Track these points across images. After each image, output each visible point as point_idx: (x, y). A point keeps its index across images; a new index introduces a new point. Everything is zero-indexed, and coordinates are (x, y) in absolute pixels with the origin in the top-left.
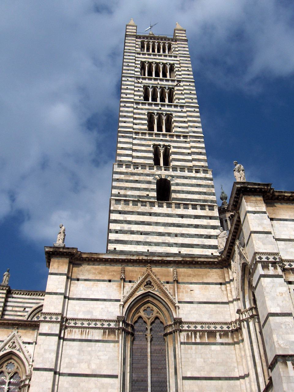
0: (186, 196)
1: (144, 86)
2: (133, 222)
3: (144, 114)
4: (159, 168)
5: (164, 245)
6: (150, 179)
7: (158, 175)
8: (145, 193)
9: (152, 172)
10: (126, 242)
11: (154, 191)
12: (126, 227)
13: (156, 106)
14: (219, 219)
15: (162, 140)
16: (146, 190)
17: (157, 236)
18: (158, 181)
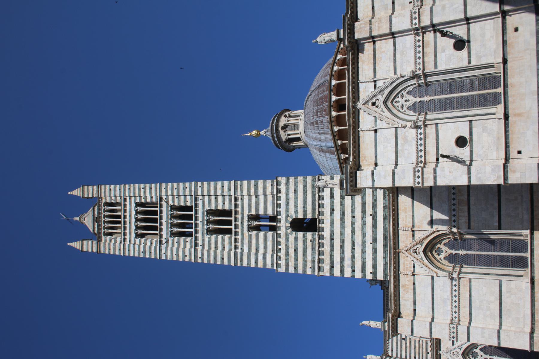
1: (171, 236)
2: (342, 256)
3: (210, 239)
4: (279, 228)
6: (292, 238)
8: (309, 244)
10: (364, 263)
12: (347, 262)
13: (198, 226)
15: (242, 223)
17: (355, 234)
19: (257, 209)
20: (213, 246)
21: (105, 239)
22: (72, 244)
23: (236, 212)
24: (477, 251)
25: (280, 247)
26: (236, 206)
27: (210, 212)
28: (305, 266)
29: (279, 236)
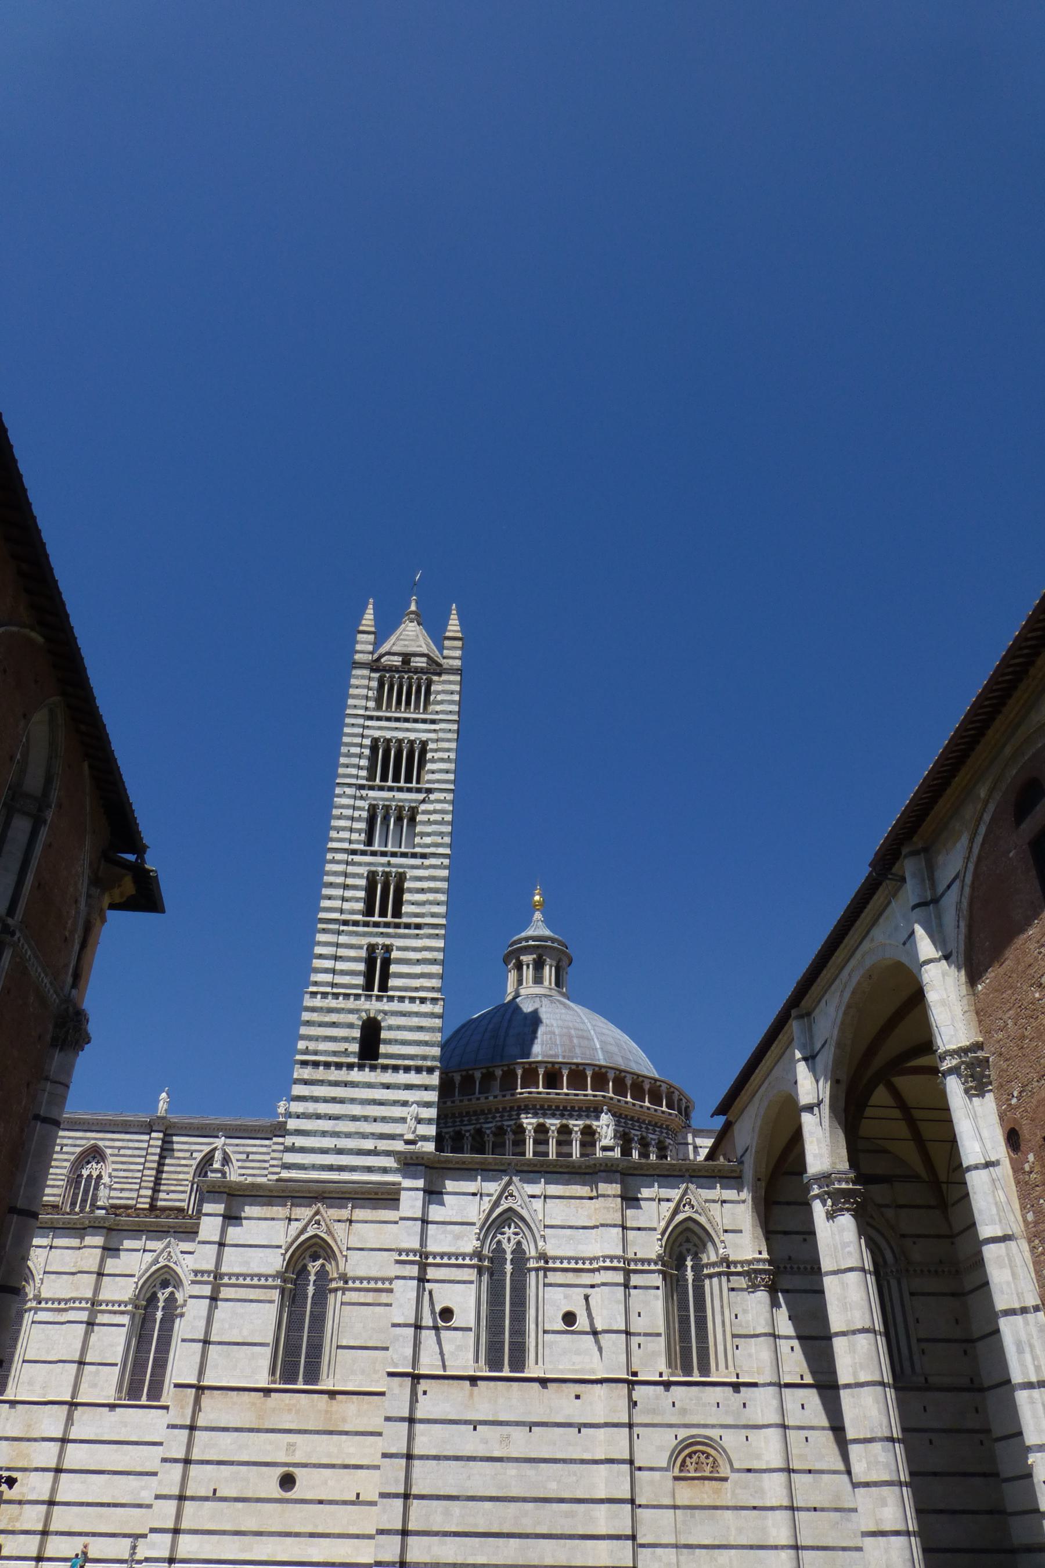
1: (370, 805)
5: (357, 1136)
6: (352, 1018)
7: (367, 1011)
8: (341, 1047)
9: (357, 1005)
12: (311, 1107)
14: (437, 1089)
15: (382, 933)
16: (345, 1039)
18: (364, 1022)
19: (400, 961)
22: (370, 609)
23: (397, 926)
24: (311, 1312)
25: (341, 998)
26: (407, 926)
27: (401, 878)
28: (310, 1038)
29: (357, 997)
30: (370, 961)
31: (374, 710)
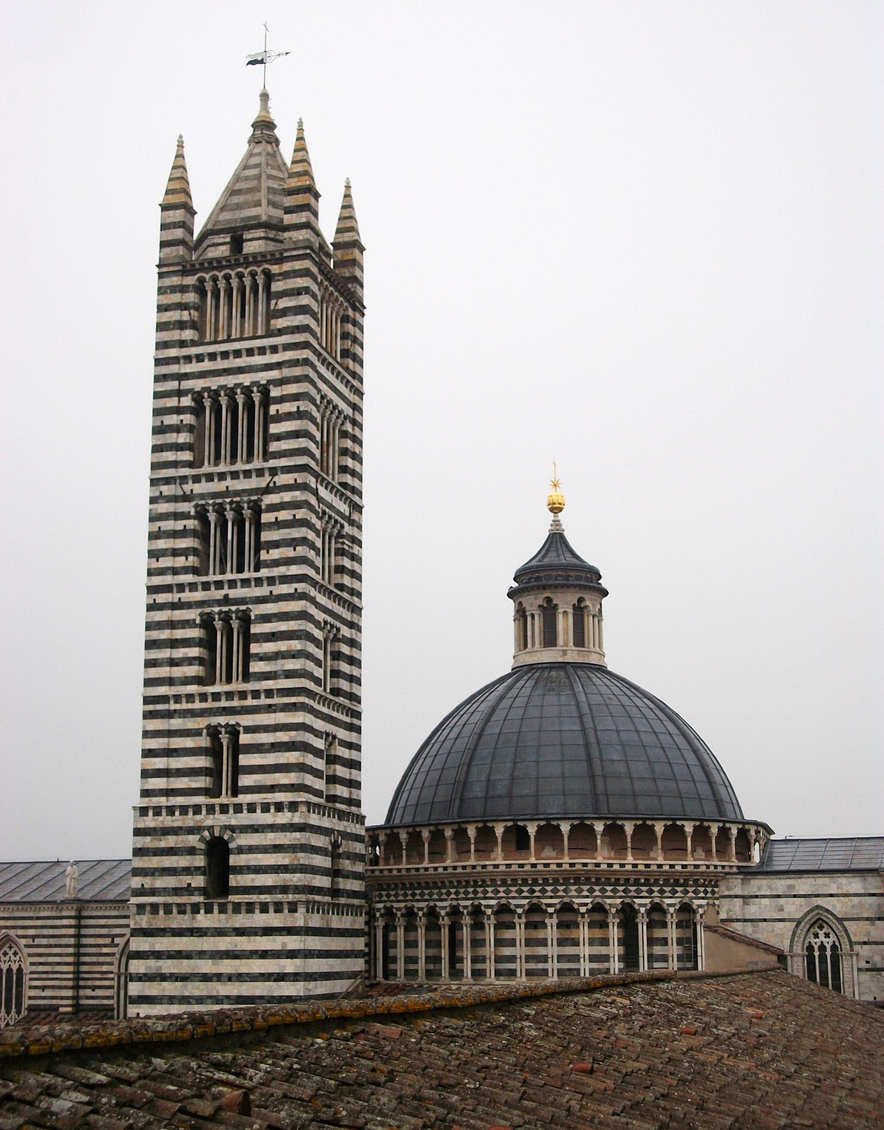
0: (253, 880)
1: (196, 506)
5: (210, 1001)
6: (193, 840)
7: (210, 828)
8: (184, 881)
9: (197, 822)
11: (199, 873)
15: (224, 708)
16: (187, 871)
18: (208, 843)
20: (179, 634)
21: (188, 286)
25: (177, 813)
27: (246, 620)
30: (214, 752)
31: (194, 343)
